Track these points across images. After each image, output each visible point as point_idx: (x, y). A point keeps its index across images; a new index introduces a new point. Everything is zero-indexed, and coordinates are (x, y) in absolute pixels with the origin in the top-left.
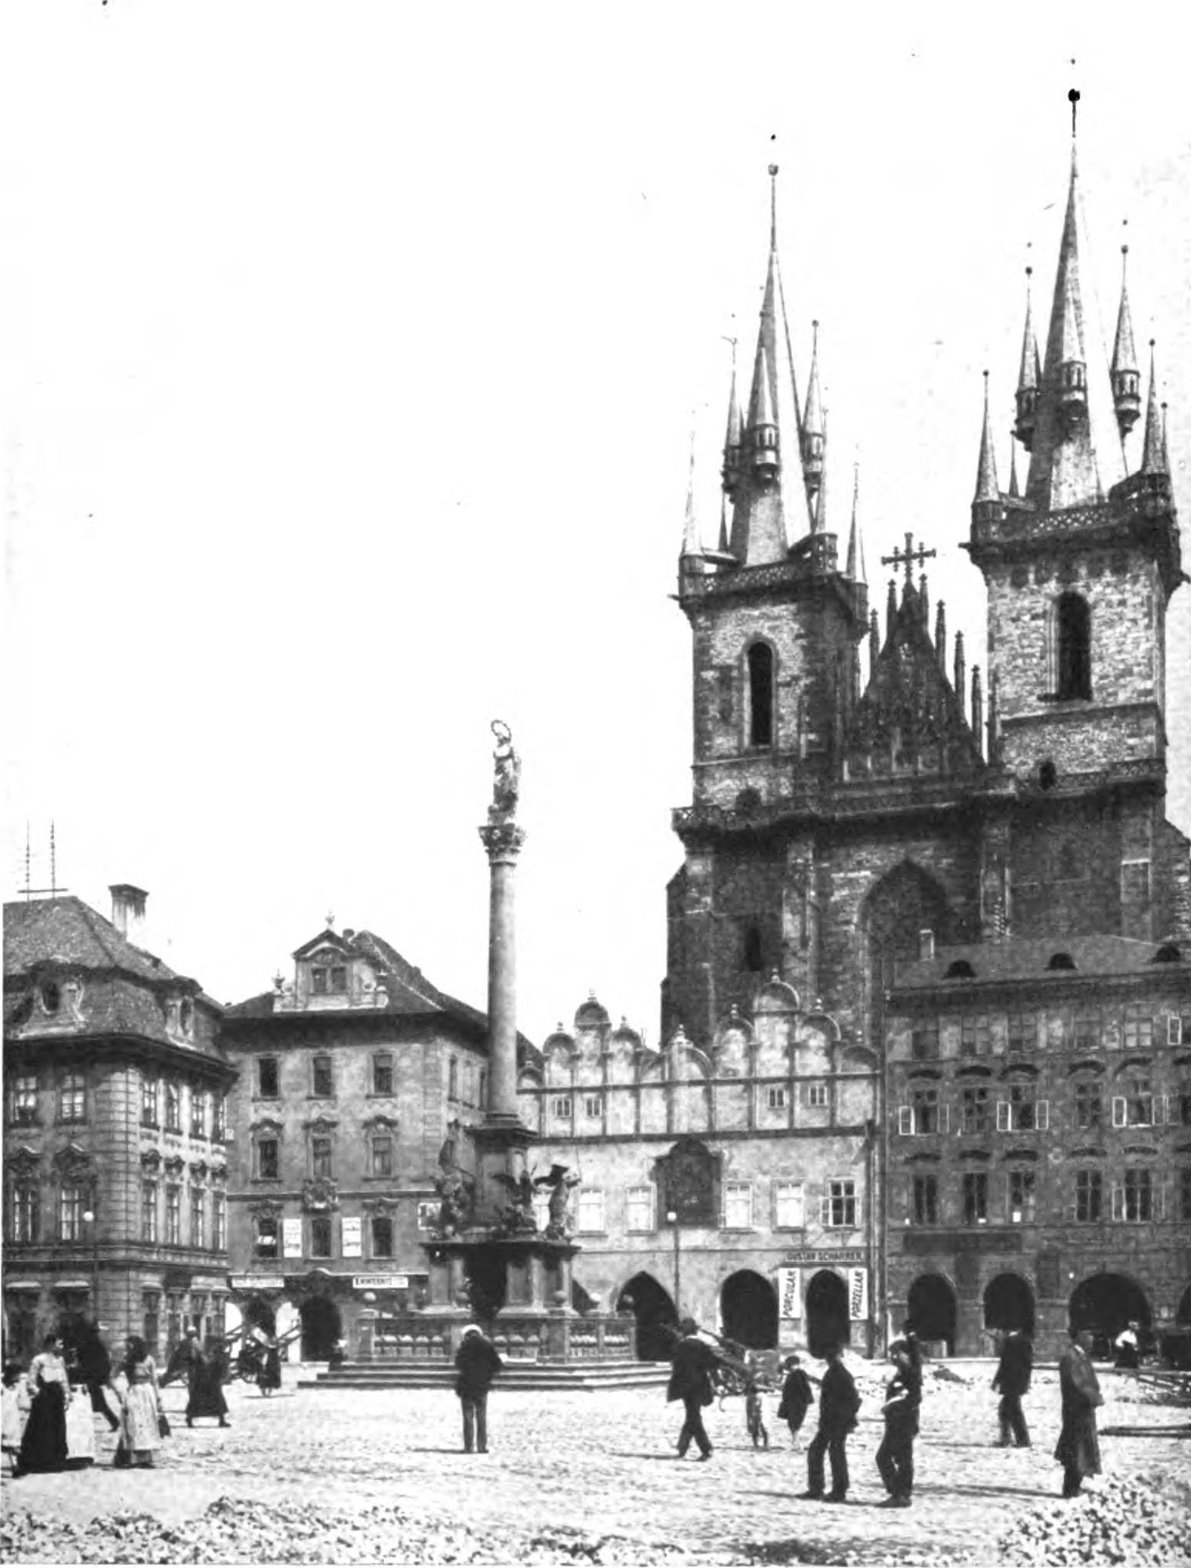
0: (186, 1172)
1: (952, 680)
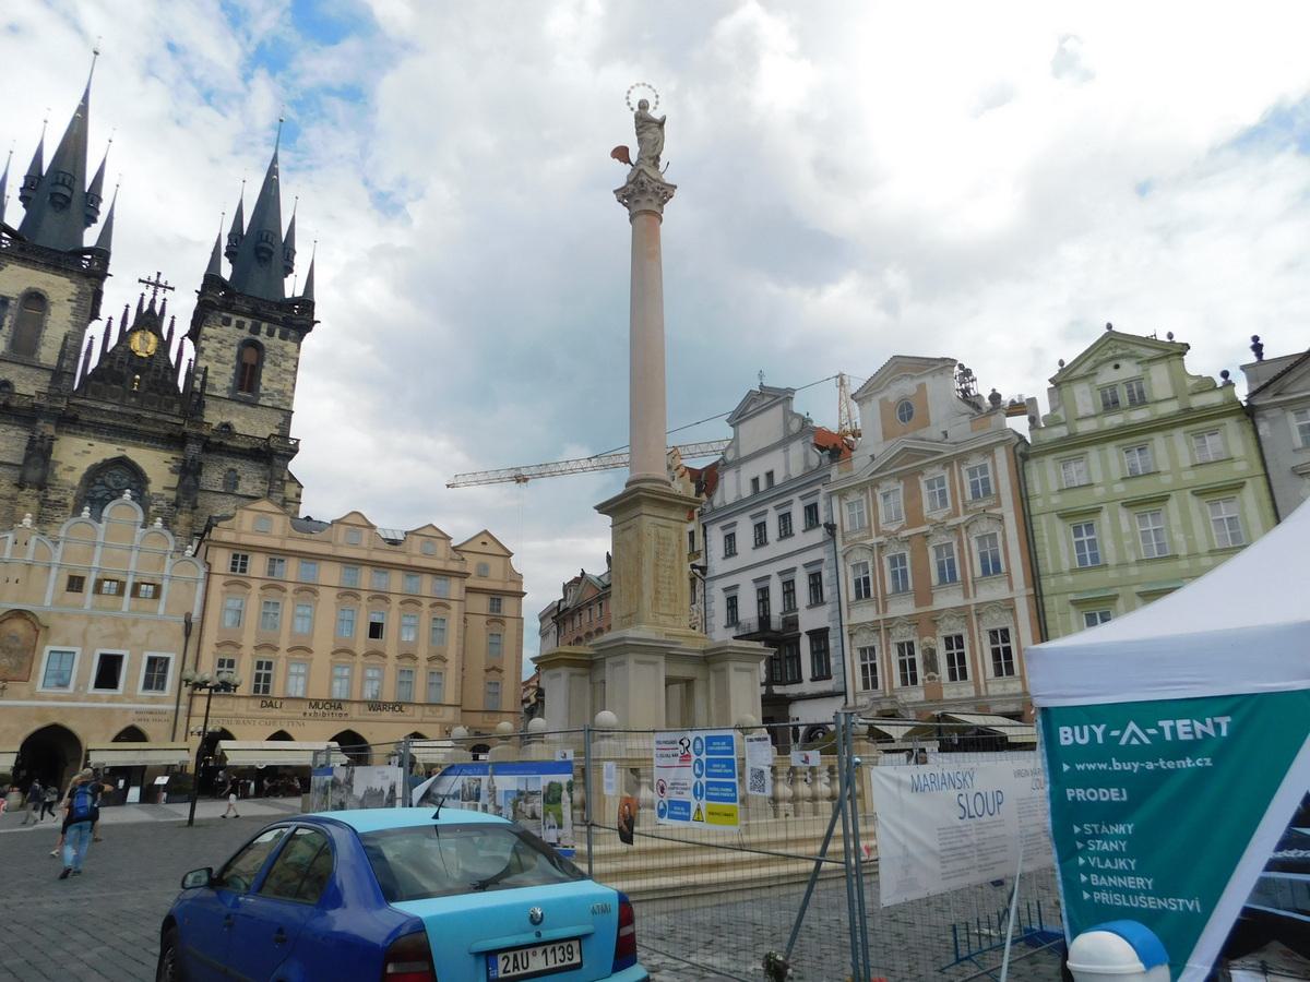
1: (173, 363)
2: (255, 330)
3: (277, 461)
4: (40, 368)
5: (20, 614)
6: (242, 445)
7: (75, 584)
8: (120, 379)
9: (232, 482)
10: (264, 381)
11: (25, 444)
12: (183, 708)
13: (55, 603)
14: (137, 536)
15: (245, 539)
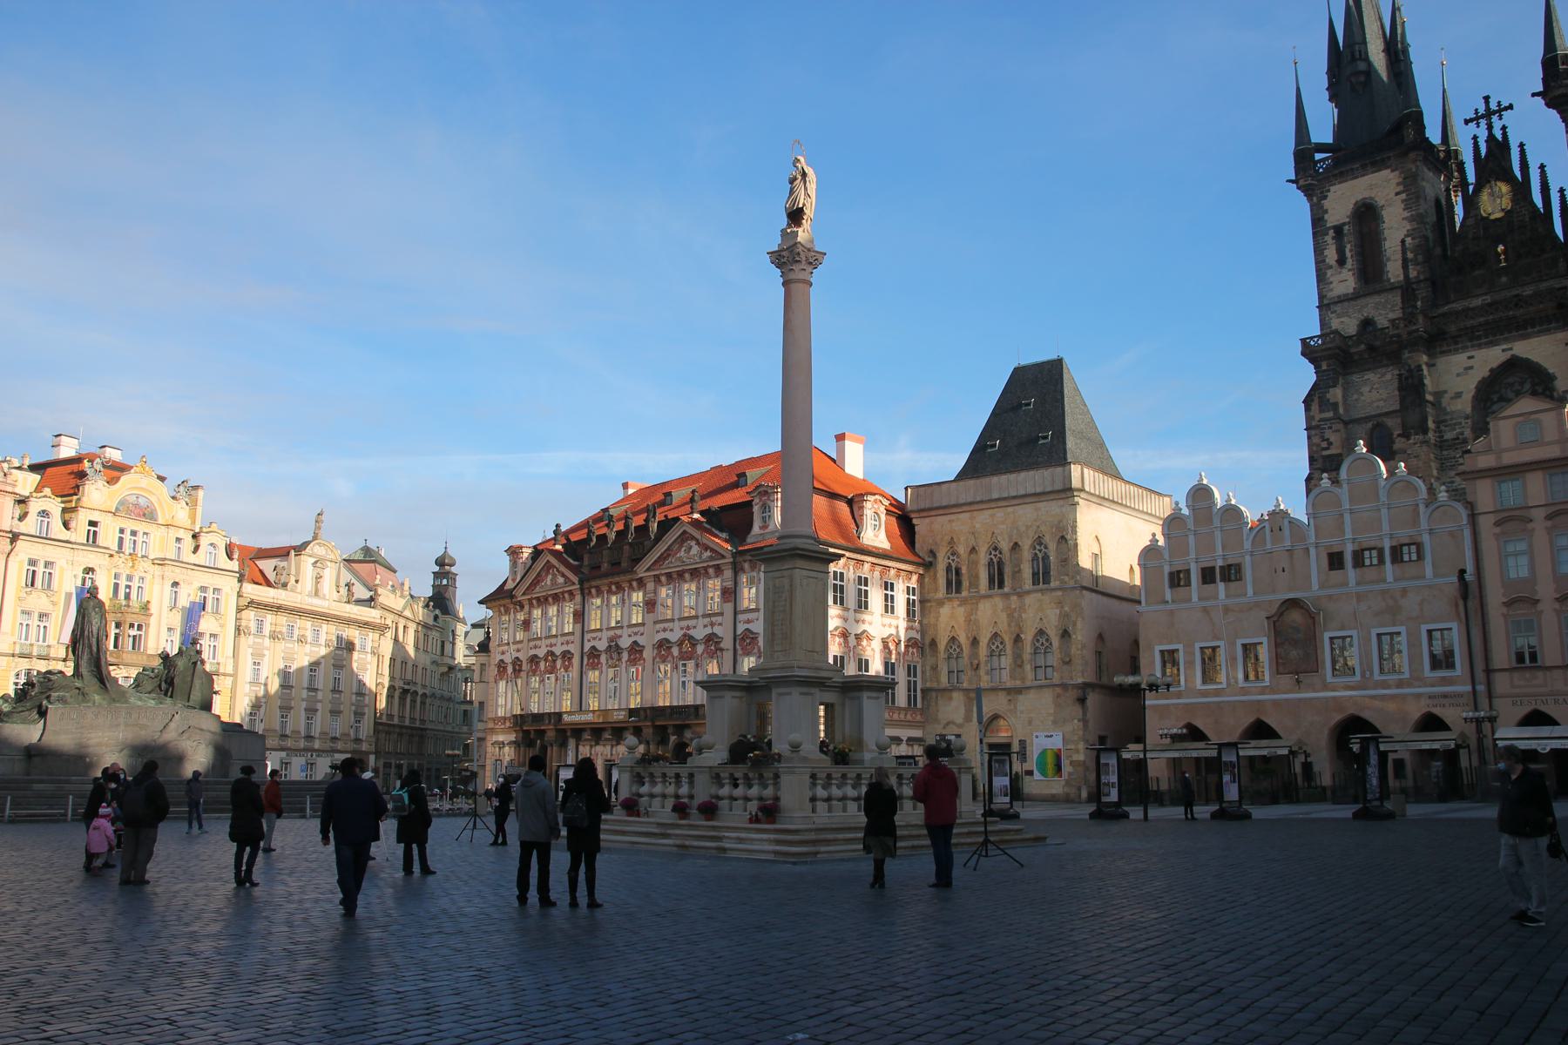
4: (1393, 288)
5: (1293, 603)
7: (1336, 561)
11: (1396, 384)
12: (1481, 688)
13: (1322, 587)
14: (1381, 492)
15: (1508, 459)
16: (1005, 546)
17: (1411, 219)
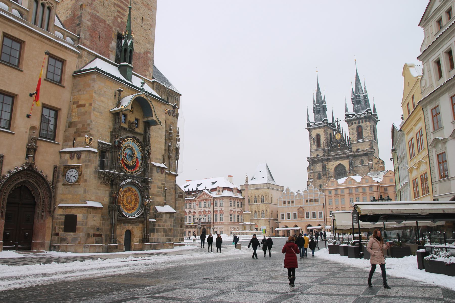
0: (236, 212)
2: (359, 123)
3: (369, 155)
5: (301, 207)
6: (361, 153)
7: (307, 201)
8: (336, 146)
9: (362, 162)
10: (364, 135)
16: (257, 196)
17: (325, 138)
